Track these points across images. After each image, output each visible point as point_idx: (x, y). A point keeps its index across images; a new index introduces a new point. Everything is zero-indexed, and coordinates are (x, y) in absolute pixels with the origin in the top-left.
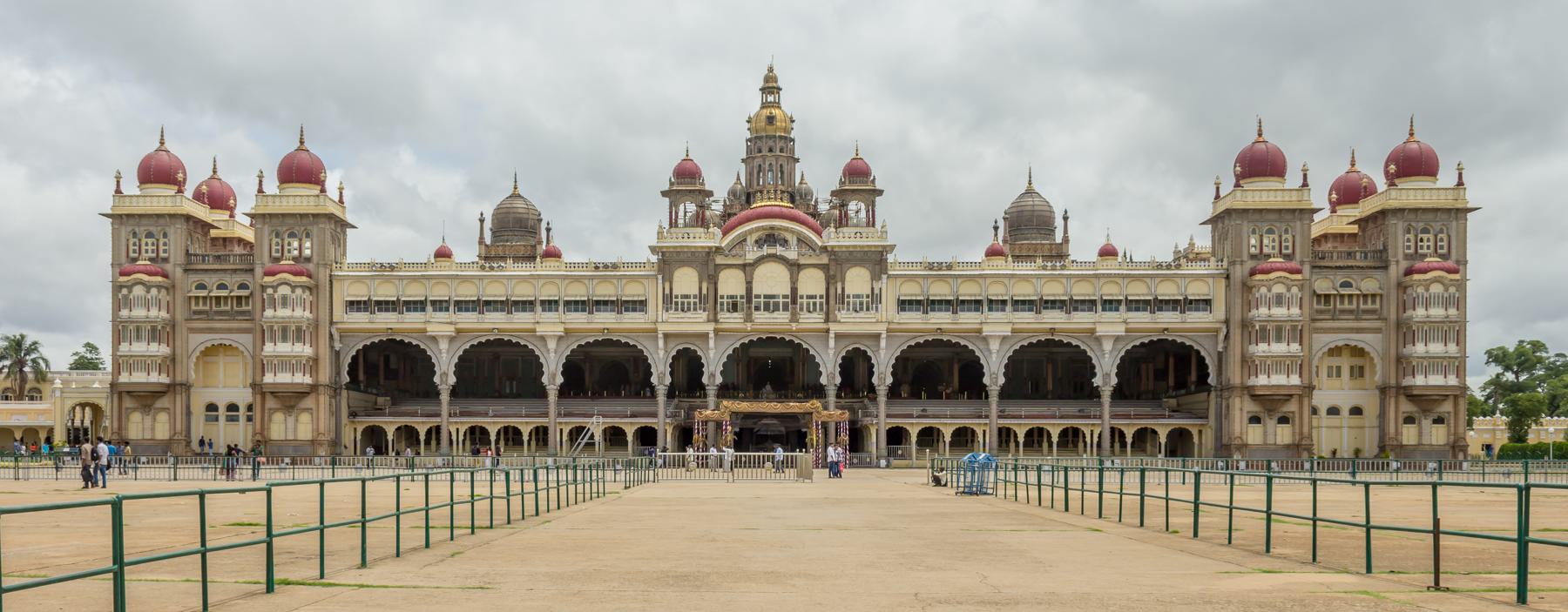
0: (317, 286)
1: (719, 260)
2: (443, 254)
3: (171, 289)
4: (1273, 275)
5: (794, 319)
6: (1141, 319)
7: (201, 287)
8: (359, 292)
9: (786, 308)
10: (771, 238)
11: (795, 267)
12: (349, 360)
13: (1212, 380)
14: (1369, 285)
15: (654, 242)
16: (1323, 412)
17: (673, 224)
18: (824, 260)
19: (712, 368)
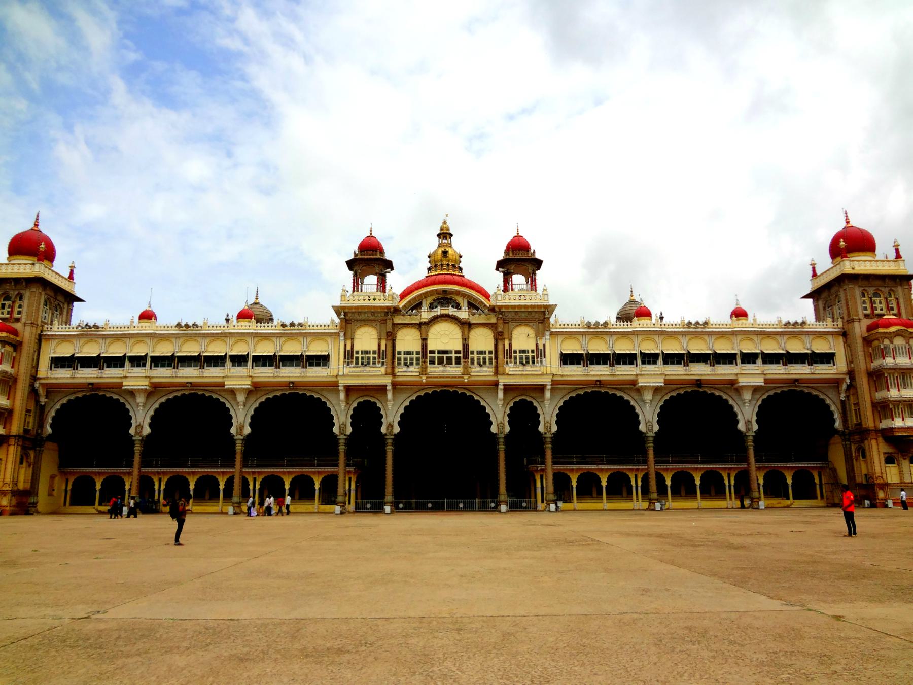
0: (21, 343)
1: (398, 320)
2: (147, 316)
5: (466, 372)
6: (777, 371)
8: (65, 351)
9: (458, 362)
10: (445, 299)
11: (466, 326)
12: (53, 413)
13: (838, 424)
15: (338, 304)
18: (494, 320)
19: (390, 419)
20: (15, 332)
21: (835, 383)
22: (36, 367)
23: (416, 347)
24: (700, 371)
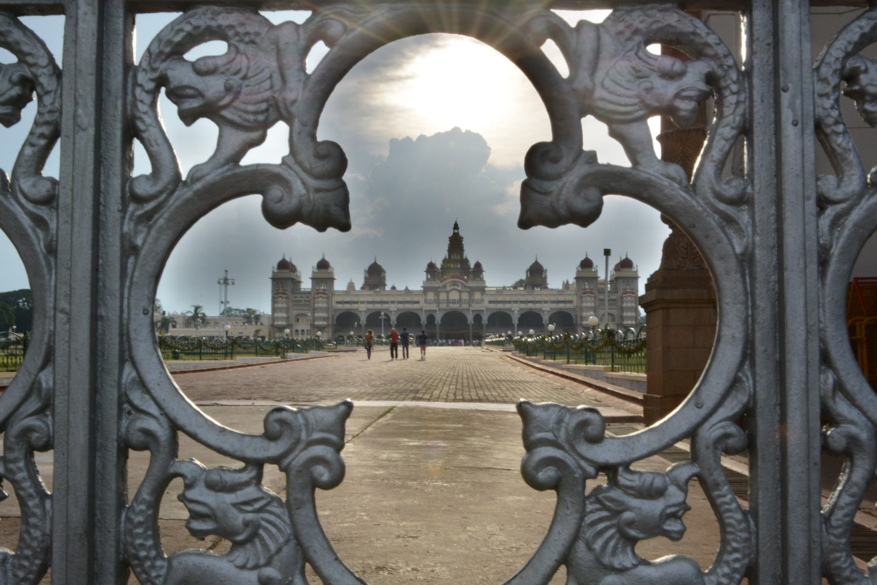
3: (287, 298)
8: (340, 299)
10: (454, 284)
11: (460, 292)
14: (613, 297)
21: (574, 309)
23: (445, 298)
24: (531, 306)
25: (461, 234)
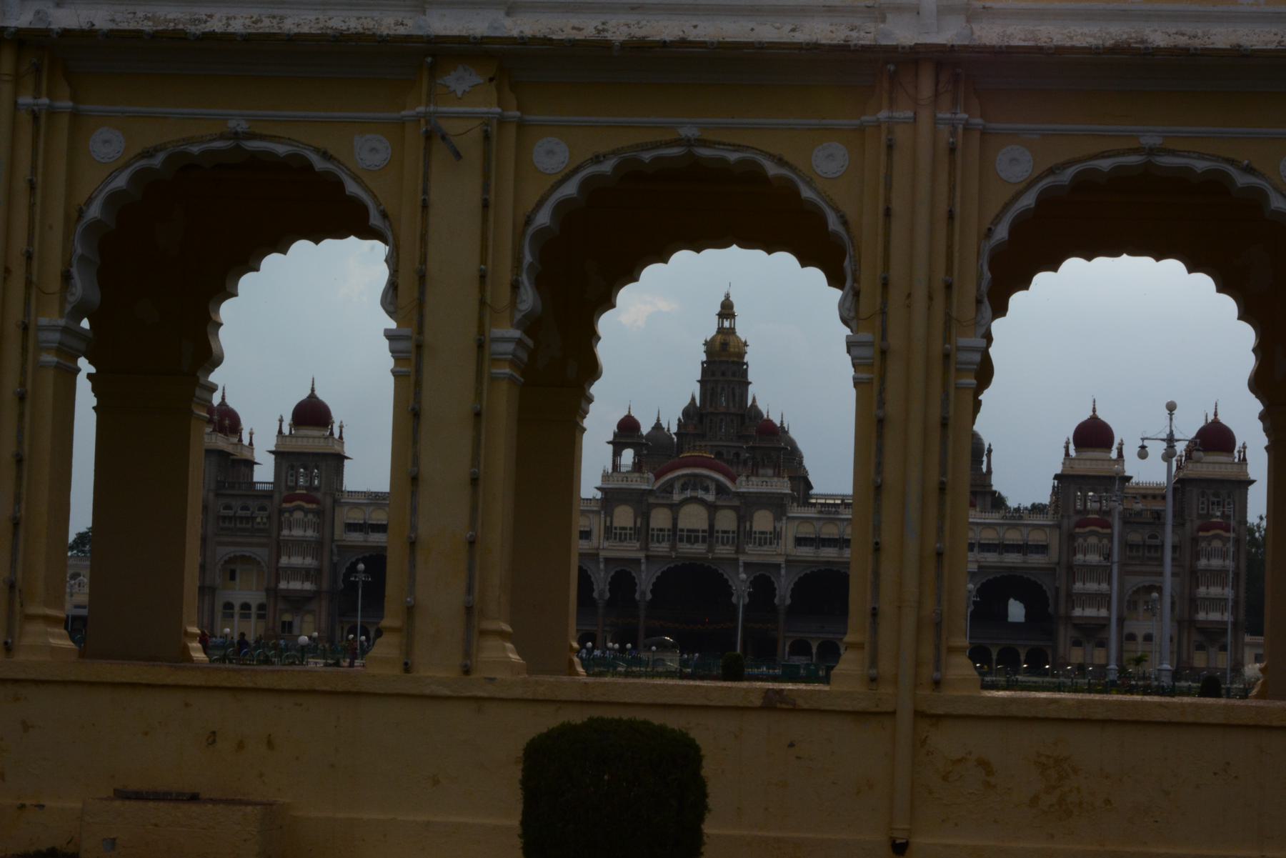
1: (651, 500)
4: (1088, 529)
5: (710, 549)
6: (991, 558)
7: (228, 507)
8: (356, 517)
9: (704, 540)
10: (693, 482)
11: (712, 508)
13: (1051, 610)
15: (599, 484)
16: (1140, 639)
17: (615, 466)
18: (736, 503)
20: (317, 502)
21: (1051, 571)
22: (333, 534)
23: (667, 524)
25: (742, 331)
